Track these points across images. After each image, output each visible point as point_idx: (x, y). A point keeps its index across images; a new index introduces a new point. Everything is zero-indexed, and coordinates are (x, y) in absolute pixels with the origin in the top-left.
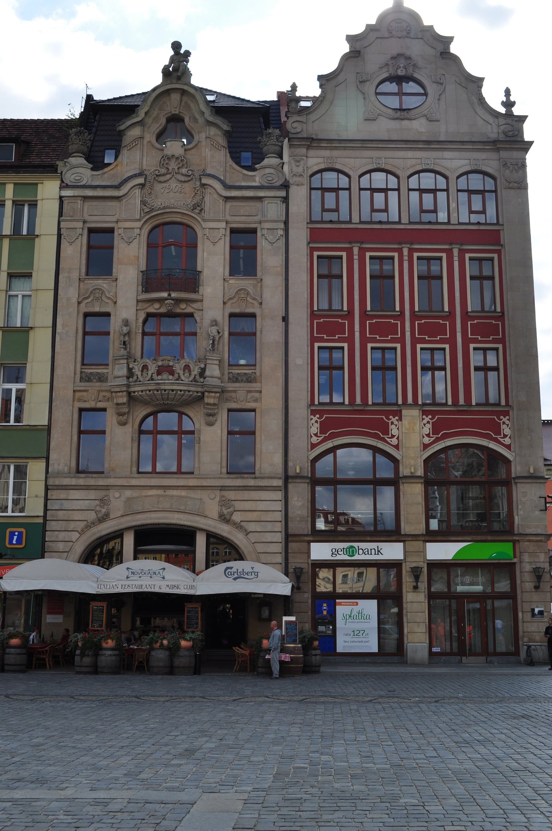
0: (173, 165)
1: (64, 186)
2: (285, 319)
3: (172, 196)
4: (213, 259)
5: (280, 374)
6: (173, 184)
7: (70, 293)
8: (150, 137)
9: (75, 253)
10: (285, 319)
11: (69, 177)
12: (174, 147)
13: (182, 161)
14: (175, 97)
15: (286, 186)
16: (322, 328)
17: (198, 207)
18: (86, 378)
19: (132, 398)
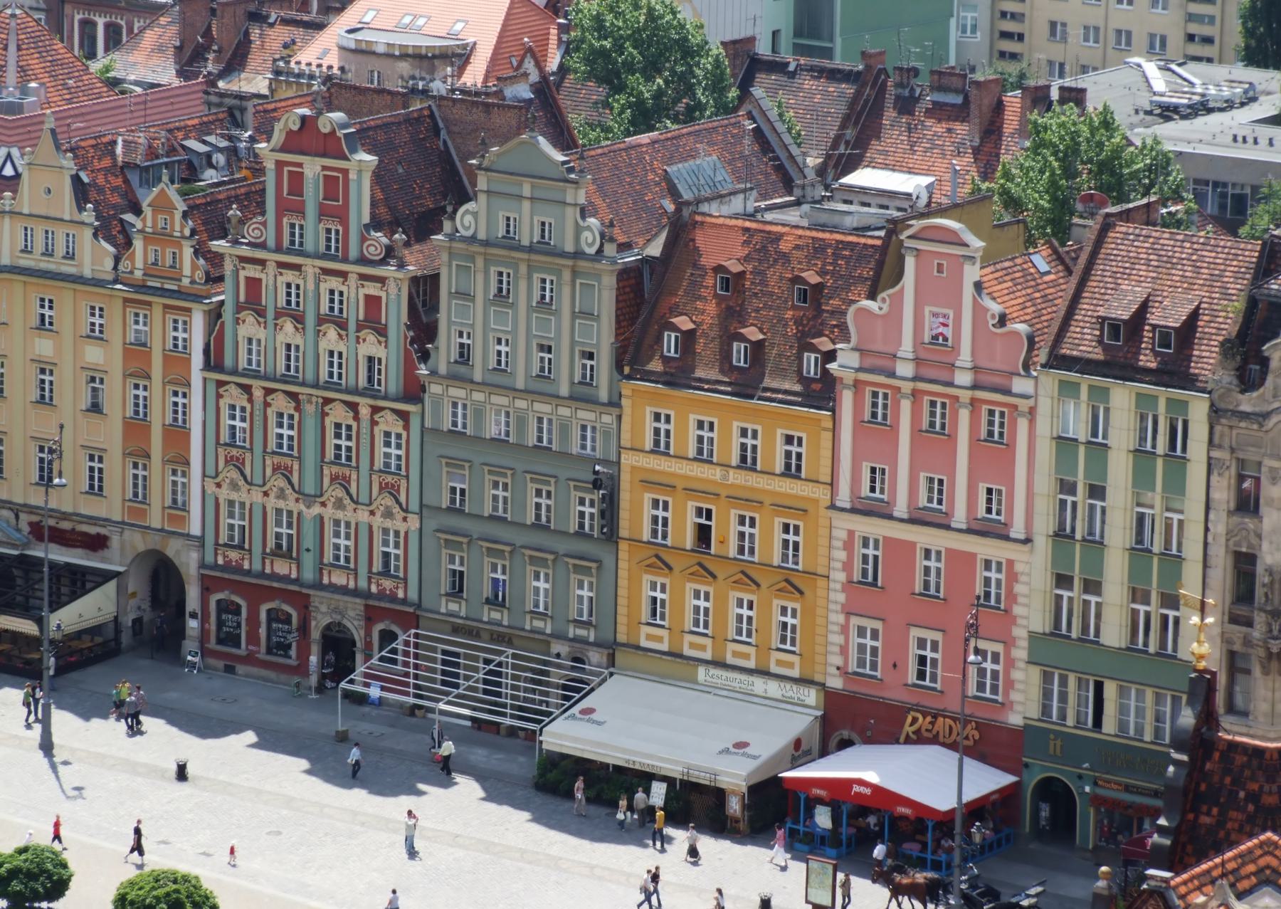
18: (1234, 619)
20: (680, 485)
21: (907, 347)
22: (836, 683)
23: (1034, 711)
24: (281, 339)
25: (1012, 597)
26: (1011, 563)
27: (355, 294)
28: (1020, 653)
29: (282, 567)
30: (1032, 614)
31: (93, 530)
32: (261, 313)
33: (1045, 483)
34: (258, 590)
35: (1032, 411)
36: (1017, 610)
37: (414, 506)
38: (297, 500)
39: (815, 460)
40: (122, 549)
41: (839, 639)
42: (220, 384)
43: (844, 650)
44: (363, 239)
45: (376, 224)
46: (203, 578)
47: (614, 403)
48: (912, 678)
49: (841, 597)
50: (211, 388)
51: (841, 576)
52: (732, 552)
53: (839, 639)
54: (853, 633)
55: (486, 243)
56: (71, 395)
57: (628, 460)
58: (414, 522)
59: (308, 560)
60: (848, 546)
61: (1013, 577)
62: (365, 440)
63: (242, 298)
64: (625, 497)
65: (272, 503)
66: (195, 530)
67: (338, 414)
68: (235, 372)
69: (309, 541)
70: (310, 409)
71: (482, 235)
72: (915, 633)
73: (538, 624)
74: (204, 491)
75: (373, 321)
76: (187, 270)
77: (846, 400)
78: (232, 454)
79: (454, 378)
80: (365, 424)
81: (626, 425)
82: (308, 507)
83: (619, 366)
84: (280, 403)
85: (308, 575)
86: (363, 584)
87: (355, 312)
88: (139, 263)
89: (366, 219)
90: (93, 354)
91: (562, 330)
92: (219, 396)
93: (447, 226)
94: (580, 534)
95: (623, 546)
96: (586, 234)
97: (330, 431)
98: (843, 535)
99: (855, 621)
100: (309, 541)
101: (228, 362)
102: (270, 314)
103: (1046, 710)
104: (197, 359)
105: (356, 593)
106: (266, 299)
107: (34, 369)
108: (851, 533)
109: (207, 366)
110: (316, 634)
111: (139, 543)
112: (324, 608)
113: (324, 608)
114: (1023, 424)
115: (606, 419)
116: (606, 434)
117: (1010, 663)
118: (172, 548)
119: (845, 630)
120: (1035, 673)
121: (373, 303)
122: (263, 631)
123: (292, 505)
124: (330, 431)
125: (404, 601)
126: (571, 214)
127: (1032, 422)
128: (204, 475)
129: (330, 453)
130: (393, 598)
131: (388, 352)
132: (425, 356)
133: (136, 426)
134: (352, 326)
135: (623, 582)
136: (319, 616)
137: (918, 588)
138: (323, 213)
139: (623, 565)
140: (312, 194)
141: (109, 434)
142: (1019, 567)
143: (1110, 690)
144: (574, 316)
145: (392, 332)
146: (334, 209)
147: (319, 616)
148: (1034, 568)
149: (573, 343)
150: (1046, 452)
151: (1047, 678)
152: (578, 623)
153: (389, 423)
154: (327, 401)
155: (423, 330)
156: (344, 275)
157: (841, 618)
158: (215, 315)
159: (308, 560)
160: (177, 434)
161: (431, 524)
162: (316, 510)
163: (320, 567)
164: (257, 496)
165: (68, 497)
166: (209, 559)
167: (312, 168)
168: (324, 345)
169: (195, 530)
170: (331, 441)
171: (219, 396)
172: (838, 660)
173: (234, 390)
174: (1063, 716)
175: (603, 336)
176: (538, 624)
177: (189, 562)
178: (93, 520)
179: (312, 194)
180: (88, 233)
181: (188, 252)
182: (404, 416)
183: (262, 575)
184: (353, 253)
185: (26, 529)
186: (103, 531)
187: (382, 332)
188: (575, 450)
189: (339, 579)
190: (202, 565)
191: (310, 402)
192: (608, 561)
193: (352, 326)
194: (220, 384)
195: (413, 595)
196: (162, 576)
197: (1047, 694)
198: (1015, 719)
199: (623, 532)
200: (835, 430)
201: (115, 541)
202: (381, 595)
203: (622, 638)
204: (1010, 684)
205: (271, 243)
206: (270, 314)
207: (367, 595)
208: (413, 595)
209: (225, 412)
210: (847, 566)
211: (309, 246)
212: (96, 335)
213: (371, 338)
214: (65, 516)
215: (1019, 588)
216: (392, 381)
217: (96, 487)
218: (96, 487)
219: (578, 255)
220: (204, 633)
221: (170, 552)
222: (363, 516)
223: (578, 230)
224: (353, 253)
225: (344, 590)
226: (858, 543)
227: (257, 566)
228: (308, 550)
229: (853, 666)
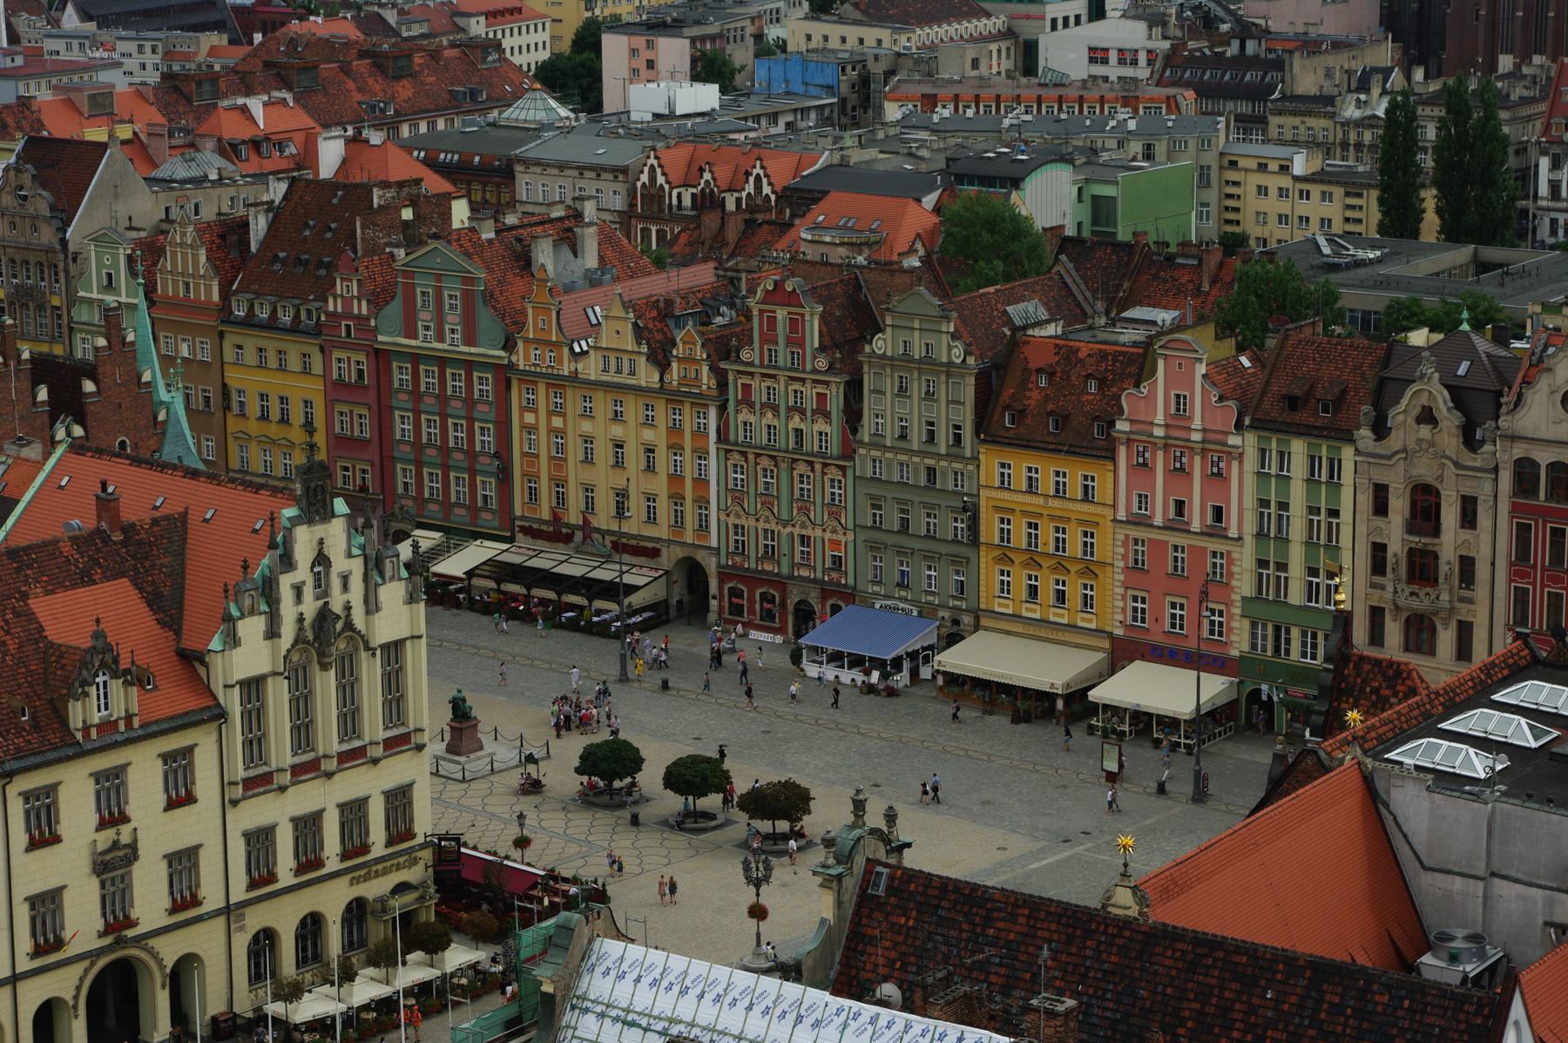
0: (1424, 446)
1: (1358, 452)
2: (1493, 564)
3: (1424, 470)
4: (1450, 515)
5: (1488, 601)
6: (1424, 459)
7: (1362, 529)
8: (1411, 421)
9: (1366, 501)
10: (1493, 564)
11: (1360, 445)
12: (1425, 431)
13: (1432, 444)
14: (1425, 394)
15: (1496, 470)
16: (1517, 573)
17: (1441, 478)
18: (1373, 586)
19: (1397, 608)
20: (1018, 508)
21: (1160, 418)
22: (1119, 632)
23: (1246, 647)
24: (764, 422)
25: (1231, 574)
26: (1229, 553)
27: (810, 393)
28: (1237, 611)
29: (768, 567)
30: (1244, 585)
31: (651, 545)
32: (751, 405)
33: (1250, 501)
34: (755, 579)
35: (1241, 455)
36: (1234, 583)
37: (850, 526)
39: (1102, 490)
41: (1120, 604)
42: (727, 451)
43: (1124, 610)
44: (814, 358)
45: (822, 348)
47: (975, 459)
48: (1167, 627)
49: (1122, 577)
50: (722, 454)
51: (1121, 564)
52: (1052, 550)
53: (1120, 604)
54: (1129, 599)
55: (892, 358)
56: (634, 458)
57: (984, 493)
58: (850, 536)
59: (785, 562)
60: (1125, 544)
61: (1231, 562)
62: (819, 485)
64: (983, 515)
65: (761, 525)
66: (714, 544)
67: (802, 468)
68: (736, 444)
69: (785, 549)
70: (784, 466)
71: (889, 353)
72: (1169, 599)
73: (930, 598)
75: (822, 412)
76: (705, 381)
77: (1122, 452)
78: (735, 495)
79: (873, 445)
80: (818, 473)
81: (982, 472)
83: (978, 435)
84: (765, 462)
85: (785, 570)
86: (819, 575)
87: (810, 404)
88: (675, 377)
89: (816, 345)
90: (648, 435)
91: (942, 415)
92: (727, 459)
93: (867, 349)
94: (955, 541)
95: (983, 548)
96: (955, 350)
97: (796, 479)
98: (1122, 537)
99: (1130, 592)
100: (785, 549)
101: (732, 437)
102: (758, 407)
103: (1254, 646)
104: (713, 436)
105: (815, 581)
106: (755, 397)
107: (610, 446)
108: (1127, 536)
109: (719, 440)
110: (790, 608)
111: (680, 553)
114: (1235, 465)
115: (970, 467)
116: (970, 478)
117: (1230, 616)
118: (700, 556)
119: (1124, 597)
120: (1246, 624)
121: (822, 397)
122: (757, 607)
123: (773, 526)
124: (796, 479)
125: (846, 586)
126: (945, 338)
127: (1241, 462)
129: (797, 494)
130: (838, 584)
131: (832, 429)
132: (855, 431)
133: (676, 479)
134: (809, 413)
135: (983, 571)
137: (1170, 570)
138: (790, 342)
139: (982, 560)
140: (782, 329)
141: (659, 485)
142: (1235, 556)
143: (1295, 633)
144: (948, 402)
145: (834, 416)
146: (796, 339)
148: (1245, 559)
149: (948, 419)
150: (1250, 481)
151: (1254, 625)
152: (955, 598)
153: (833, 473)
154: (794, 461)
155: (853, 416)
156: (803, 380)
157: (1120, 591)
158: (723, 408)
159: (785, 562)
160: (701, 482)
161: (861, 536)
162: (789, 529)
163: (793, 566)
164: (752, 522)
165: (634, 525)
166: (723, 561)
167: (781, 314)
168: (791, 425)
169: (714, 544)
170: (797, 485)
171: (727, 459)
172: (1120, 617)
173: (737, 456)
174: (1264, 650)
175: (966, 416)
176: (930, 598)
177: (711, 564)
179: (782, 329)
180: (643, 359)
181: (705, 369)
182: (843, 469)
184: (809, 367)
185: (609, 545)
187: (827, 416)
188: (951, 487)
189: (804, 573)
190: (719, 566)
192: (973, 557)
193: (809, 413)
194: (727, 451)
195: (851, 582)
196: (693, 572)
197: (1254, 636)
198: (1235, 653)
199: (982, 540)
200: (1115, 471)
201: (664, 552)
202: (831, 582)
203: (983, 606)
204: (1230, 630)
205: (757, 362)
206: (758, 407)
208: (851, 582)
209: (730, 469)
210: (1125, 557)
211: (781, 363)
212: (649, 422)
213: (821, 420)
214: (633, 537)
215: (1235, 569)
216: (834, 448)
217: (651, 518)
218: (651, 518)
219: (950, 364)
220: (721, 608)
221: (699, 558)
222: (818, 532)
223: (950, 348)
224: (809, 367)
225: (807, 580)
226: (1131, 543)
227: (753, 566)
229: (1129, 621)
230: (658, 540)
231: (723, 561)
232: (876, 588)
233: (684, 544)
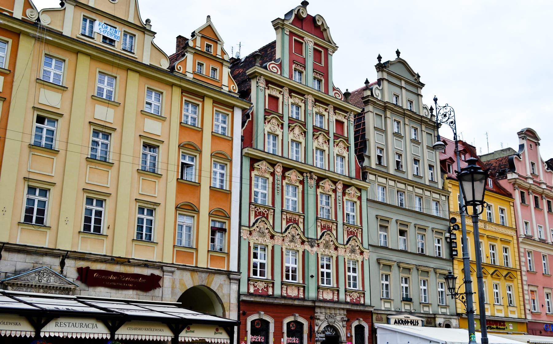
29: (293, 292)
31: (147, 272)
38: (303, 242)
40: (173, 288)
46: (240, 303)
63: (267, 107)
66: (234, 267)
74: (240, 237)
82: (312, 246)
85: (312, 294)
86: (342, 297)
111: (188, 281)
112: (322, 318)
113: (322, 318)
128: (240, 225)
136: (320, 323)
147: (320, 323)
161: (374, 257)
162: (315, 249)
165: (119, 242)
178: (146, 264)
183: (282, 297)
186: (157, 272)
189: (328, 296)
191: (311, 178)
194: (254, 160)
201: (167, 281)
207: (346, 303)
221: (214, 286)
227: (277, 292)
228: (312, 276)
230: (160, 266)
231: (244, 289)
232: (387, 305)
233: (195, 270)
